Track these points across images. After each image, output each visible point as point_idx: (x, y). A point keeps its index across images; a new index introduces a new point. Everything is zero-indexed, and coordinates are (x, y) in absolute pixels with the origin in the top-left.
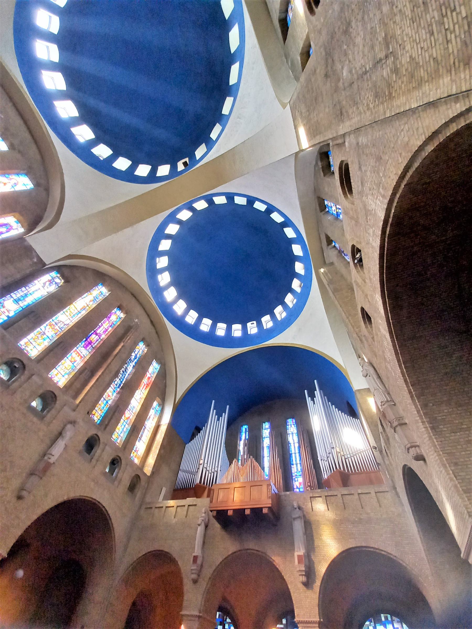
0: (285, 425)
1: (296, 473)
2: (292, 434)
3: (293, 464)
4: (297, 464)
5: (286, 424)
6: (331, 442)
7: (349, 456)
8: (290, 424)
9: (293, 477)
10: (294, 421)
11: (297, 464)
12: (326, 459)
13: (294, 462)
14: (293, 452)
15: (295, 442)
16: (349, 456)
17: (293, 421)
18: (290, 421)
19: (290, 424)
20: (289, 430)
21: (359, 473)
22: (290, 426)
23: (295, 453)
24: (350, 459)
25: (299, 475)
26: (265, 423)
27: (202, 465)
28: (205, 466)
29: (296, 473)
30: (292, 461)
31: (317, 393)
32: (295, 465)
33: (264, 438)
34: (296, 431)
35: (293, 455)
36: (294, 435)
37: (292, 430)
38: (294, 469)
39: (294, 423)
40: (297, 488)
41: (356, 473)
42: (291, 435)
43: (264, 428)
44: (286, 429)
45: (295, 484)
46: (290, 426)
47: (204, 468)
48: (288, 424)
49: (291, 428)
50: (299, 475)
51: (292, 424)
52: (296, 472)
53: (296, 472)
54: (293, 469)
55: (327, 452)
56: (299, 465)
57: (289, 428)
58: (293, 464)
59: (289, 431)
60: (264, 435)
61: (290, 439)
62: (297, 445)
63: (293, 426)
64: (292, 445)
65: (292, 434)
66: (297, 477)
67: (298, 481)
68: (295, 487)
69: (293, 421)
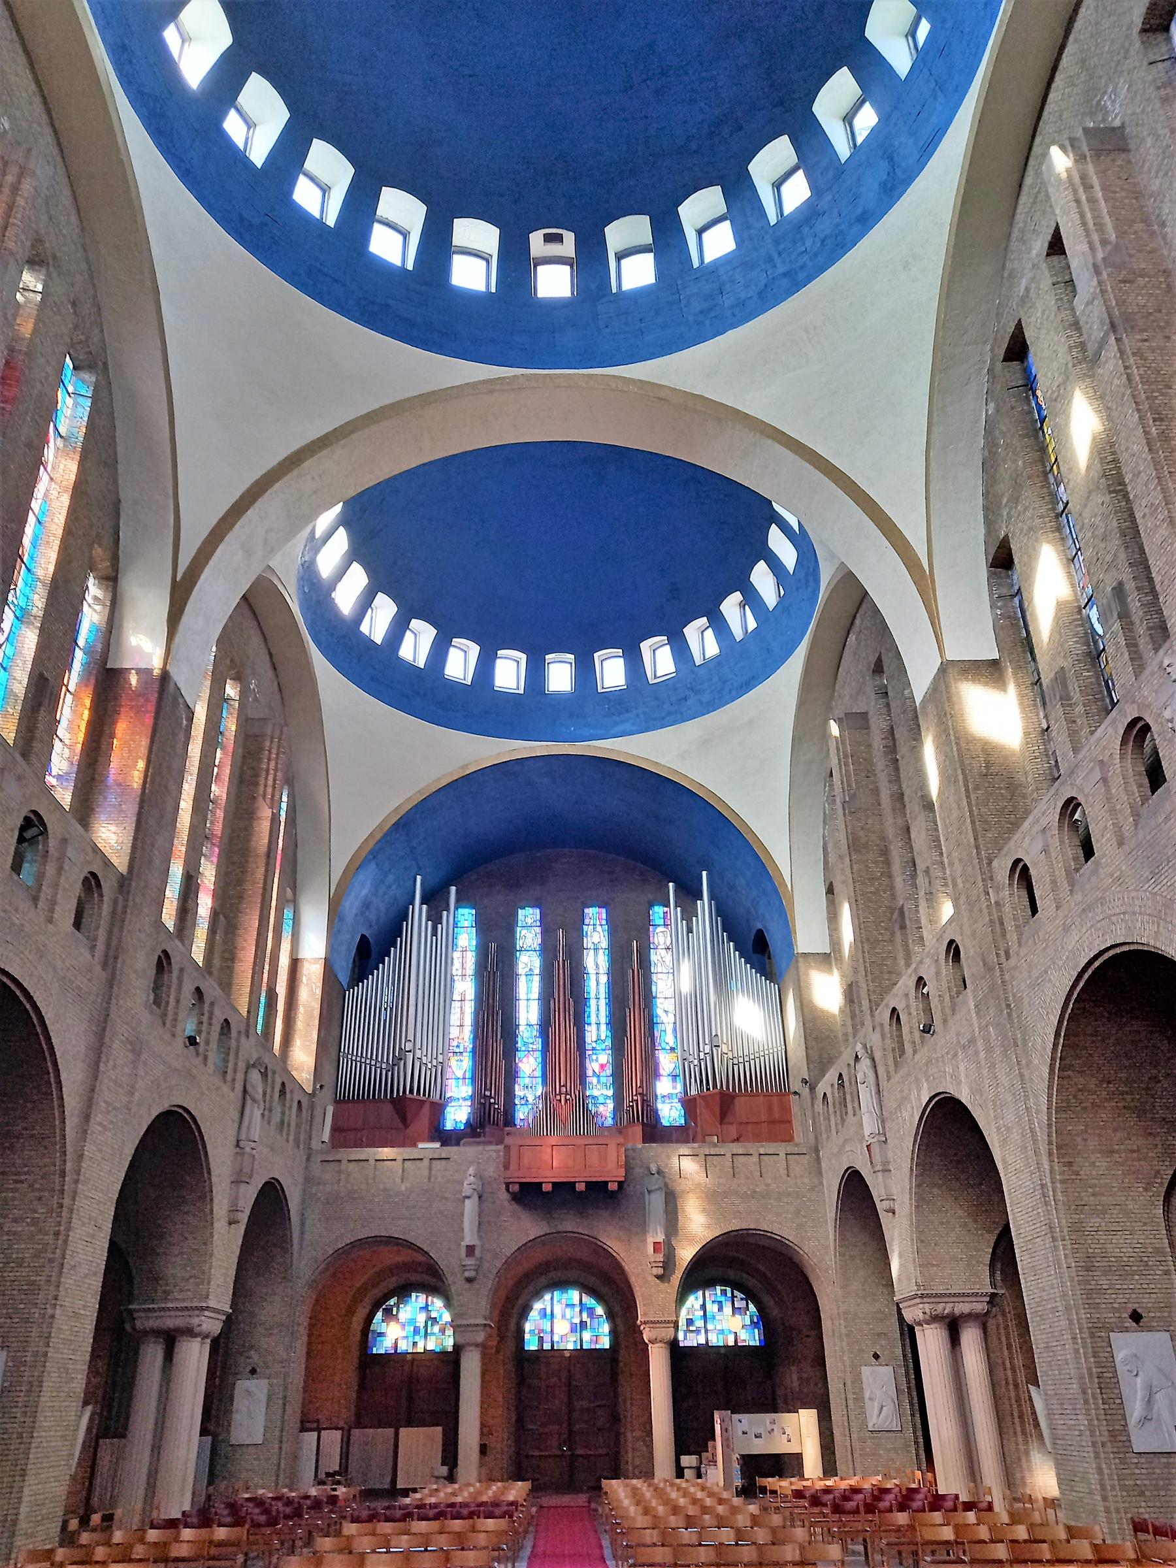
0: (576, 929)
6: (714, 1034)
7: (741, 1060)
10: (604, 916)
12: (696, 1062)
16: (741, 1060)
18: (591, 912)
21: (752, 1095)
22: (591, 927)
24: (741, 1066)
27: (411, 1054)
28: (418, 1054)
31: (704, 906)
39: (604, 922)
41: (746, 1094)
47: (416, 1060)
48: (587, 921)
51: (598, 923)
55: (701, 1049)
63: (599, 928)
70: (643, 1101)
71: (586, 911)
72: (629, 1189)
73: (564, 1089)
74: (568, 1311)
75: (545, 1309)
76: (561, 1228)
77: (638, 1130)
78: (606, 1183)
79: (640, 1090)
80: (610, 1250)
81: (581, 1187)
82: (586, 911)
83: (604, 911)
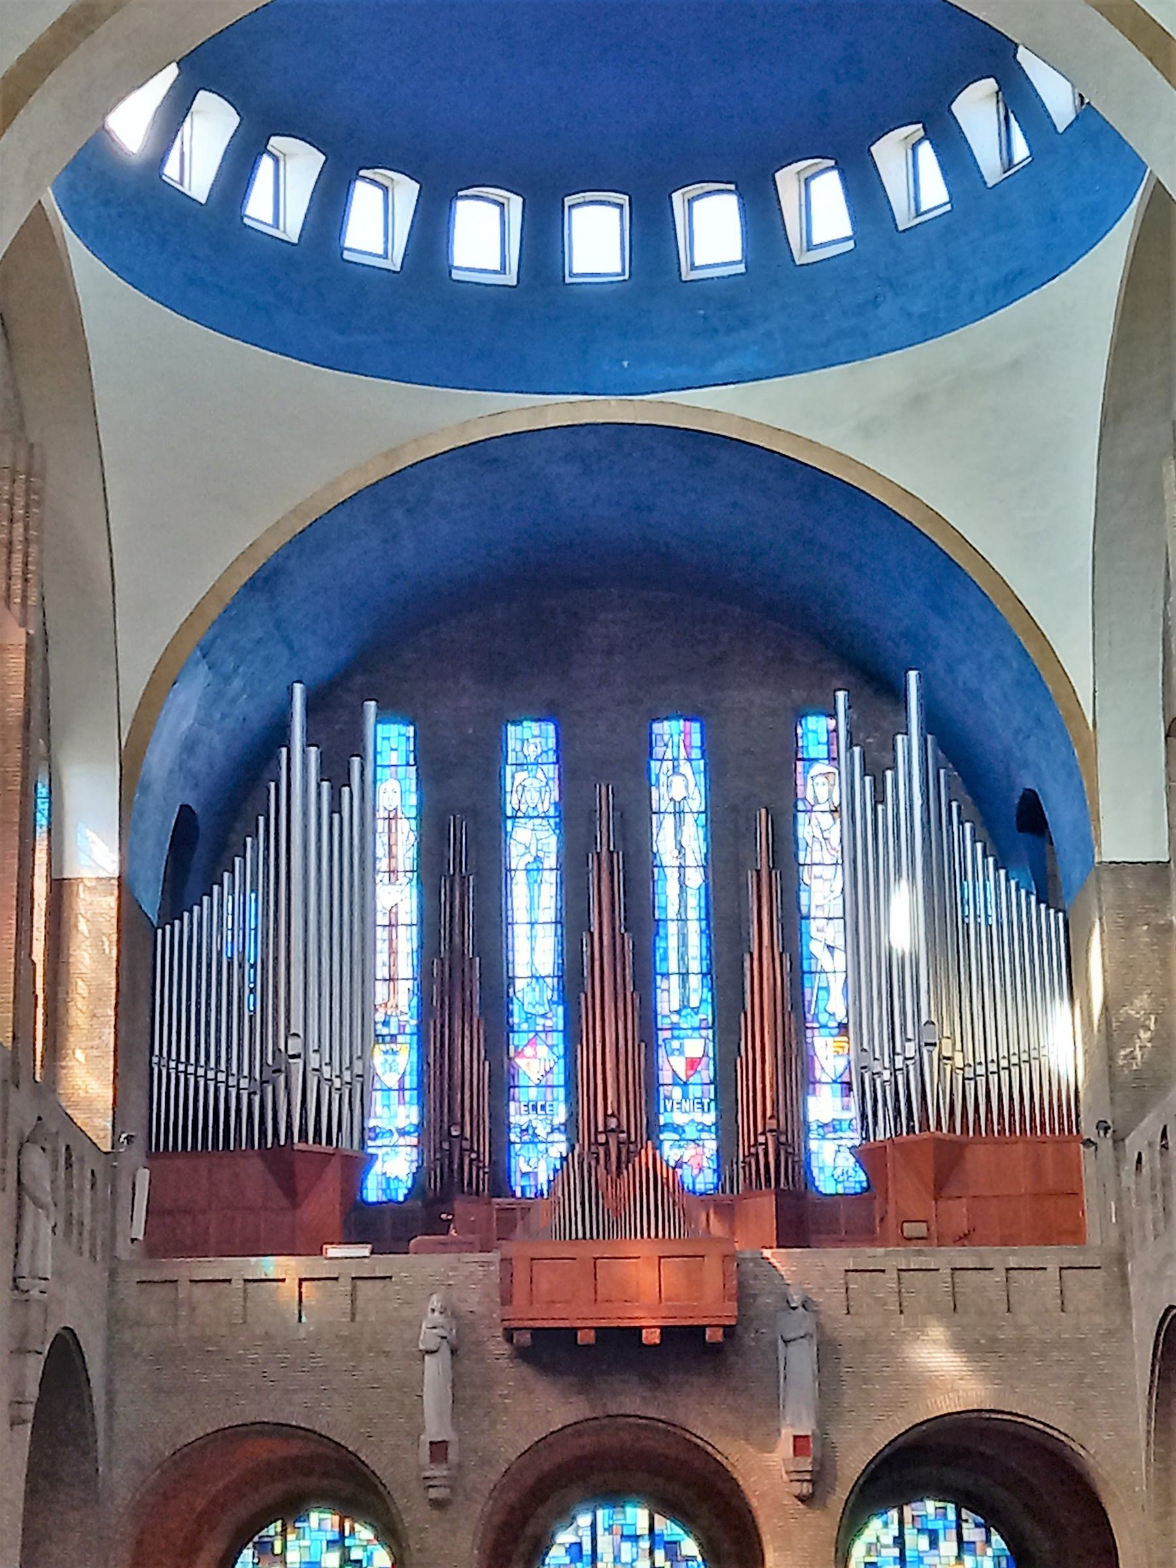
1: (675, 1018)
2: (679, 813)
3: (666, 975)
4: (684, 976)
5: (646, 749)
8: (669, 755)
9: (662, 1035)
10: (696, 739)
11: (684, 976)
13: (673, 966)
14: (672, 912)
15: (690, 860)
17: (687, 734)
19: (669, 755)
20: (663, 790)
22: (668, 765)
23: (683, 920)
25: (693, 1029)
26: (517, 722)
29: (675, 1018)
30: (665, 958)
32: (675, 980)
33: (514, 817)
34: (697, 802)
35: (673, 928)
36: (689, 819)
37: (678, 792)
38: (668, 998)
39: (696, 754)
40: (674, 1084)
42: (669, 821)
43: (511, 758)
44: (643, 782)
45: (666, 1066)
46: (668, 765)
48: (658, 751)
49: (677, 781)
50: (693, 1029)
51: (683, 754)
52: (678, 1012)
53: (678, 1012)
54: (661, 996)
56: (694, 981)
57: (663, 778)
58: (666, 975)
59: (661, 798)
60: (511, 802)
61: (664, 842)
62: (695, 878)
63: (685, 768)
64: (672, 874)
65: (679, 813)
66: (682, 1033)
67: (681, 1051)
68: (665, 1076)
69: (687, 734)
70: (778, 1144)
71: (657, 727)
72: (749, 1338)
73: (613, 1123)
74: (626, 1547)
75: (580, 1544)
76: (613, 1409)
77: (766, 1205)
78: (702, 1329)
79: (772, 1124)
80: (709, 1449)
81: (652, 1337)
82: (657, 727)
83: (696, 727)
